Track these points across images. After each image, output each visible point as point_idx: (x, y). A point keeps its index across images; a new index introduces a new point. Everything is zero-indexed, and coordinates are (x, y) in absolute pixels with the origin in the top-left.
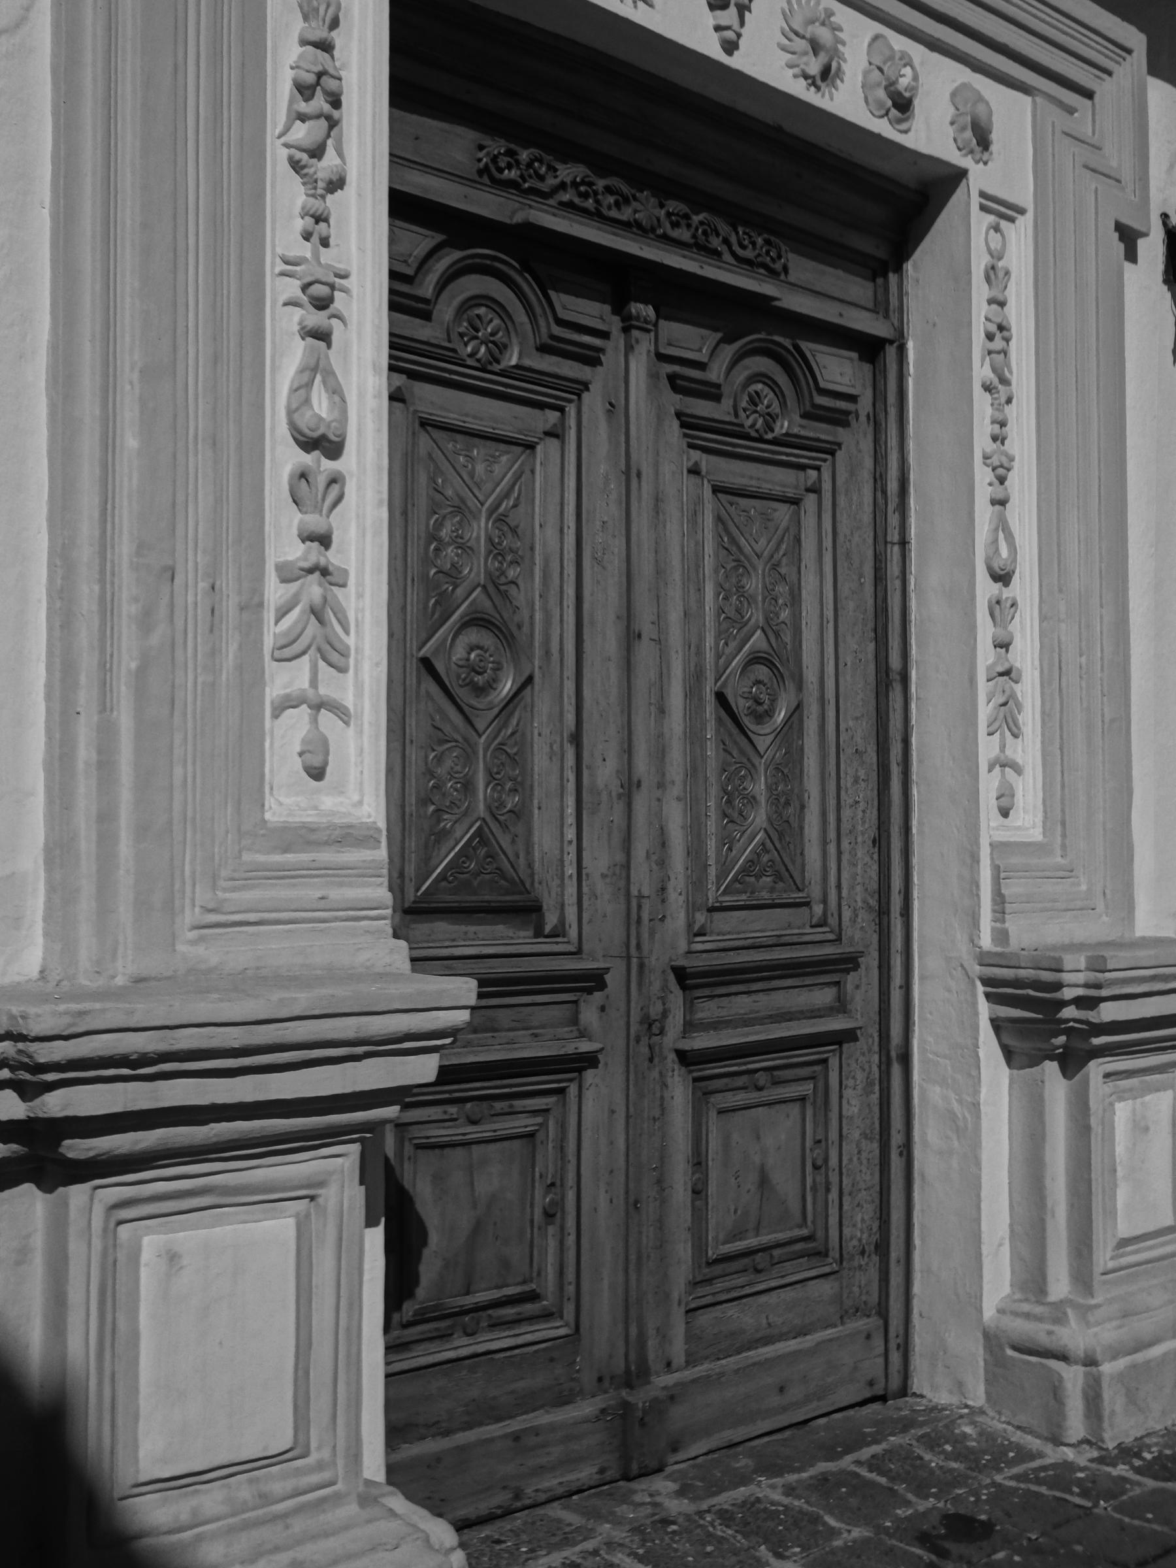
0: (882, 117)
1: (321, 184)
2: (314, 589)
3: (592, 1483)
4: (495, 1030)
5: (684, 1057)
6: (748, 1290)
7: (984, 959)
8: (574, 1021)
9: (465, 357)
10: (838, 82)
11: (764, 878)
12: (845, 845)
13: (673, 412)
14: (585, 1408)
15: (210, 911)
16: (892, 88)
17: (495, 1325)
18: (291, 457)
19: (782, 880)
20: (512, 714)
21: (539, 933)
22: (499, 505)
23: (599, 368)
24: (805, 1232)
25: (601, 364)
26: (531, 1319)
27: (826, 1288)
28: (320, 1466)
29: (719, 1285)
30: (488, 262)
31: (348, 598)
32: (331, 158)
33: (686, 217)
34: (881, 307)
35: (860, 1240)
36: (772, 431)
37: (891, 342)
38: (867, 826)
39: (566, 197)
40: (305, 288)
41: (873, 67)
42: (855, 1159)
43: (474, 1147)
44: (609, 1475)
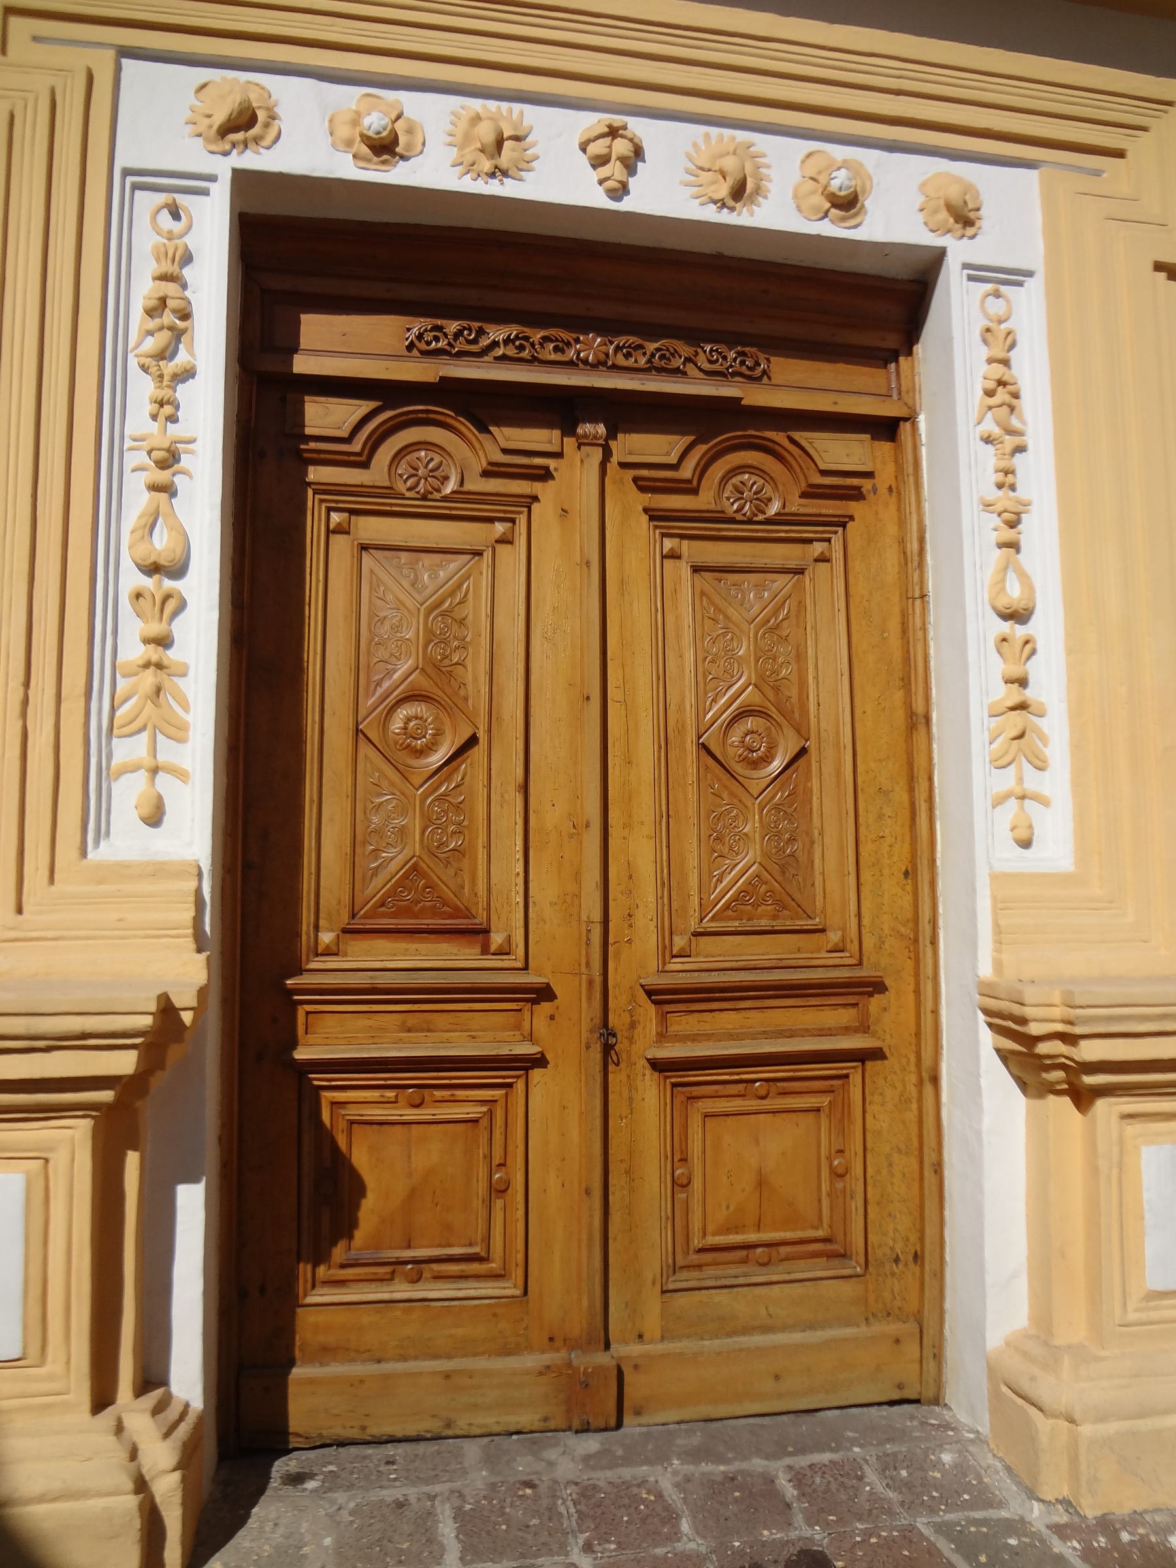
0: (822, 219)
1: (166, 378)
2: (149, 678)
3: (533, 1428)
4: (429, 1030)
5: (659, 1066)
6: (741, 1281)
8: (518, 1027)
9: (404, 491)
10: (760, 199)
11: (763, 907)
12: (866, 876)
13: (640, 508)
14: (531, 1361)
15: (11, 929)
16: (826, 192)
17: (438, 1277)
18: (131, 579)
19: (785, 908)
20: (457, 769)
21: (485, 950)
22: (442, 602)
23: (551, 482)
24: (820, 1233)
25: (552, 478)
26: (477, 1277)
27: (847, 1289)
28: (51, 1378)
29: (710, 1272)
30: (425, 416)
31: (185, 685)
32: (182, 358)
33: (641, 347)
35: (892, 1249)
36: (763, 513)
37: (906, 419)
38: (895, 859)
39: (500, 352)
40: (149, 453)
41: (806, 179)
42: (884, 1172)
43: (414, 1126)
44: (552, 1424)
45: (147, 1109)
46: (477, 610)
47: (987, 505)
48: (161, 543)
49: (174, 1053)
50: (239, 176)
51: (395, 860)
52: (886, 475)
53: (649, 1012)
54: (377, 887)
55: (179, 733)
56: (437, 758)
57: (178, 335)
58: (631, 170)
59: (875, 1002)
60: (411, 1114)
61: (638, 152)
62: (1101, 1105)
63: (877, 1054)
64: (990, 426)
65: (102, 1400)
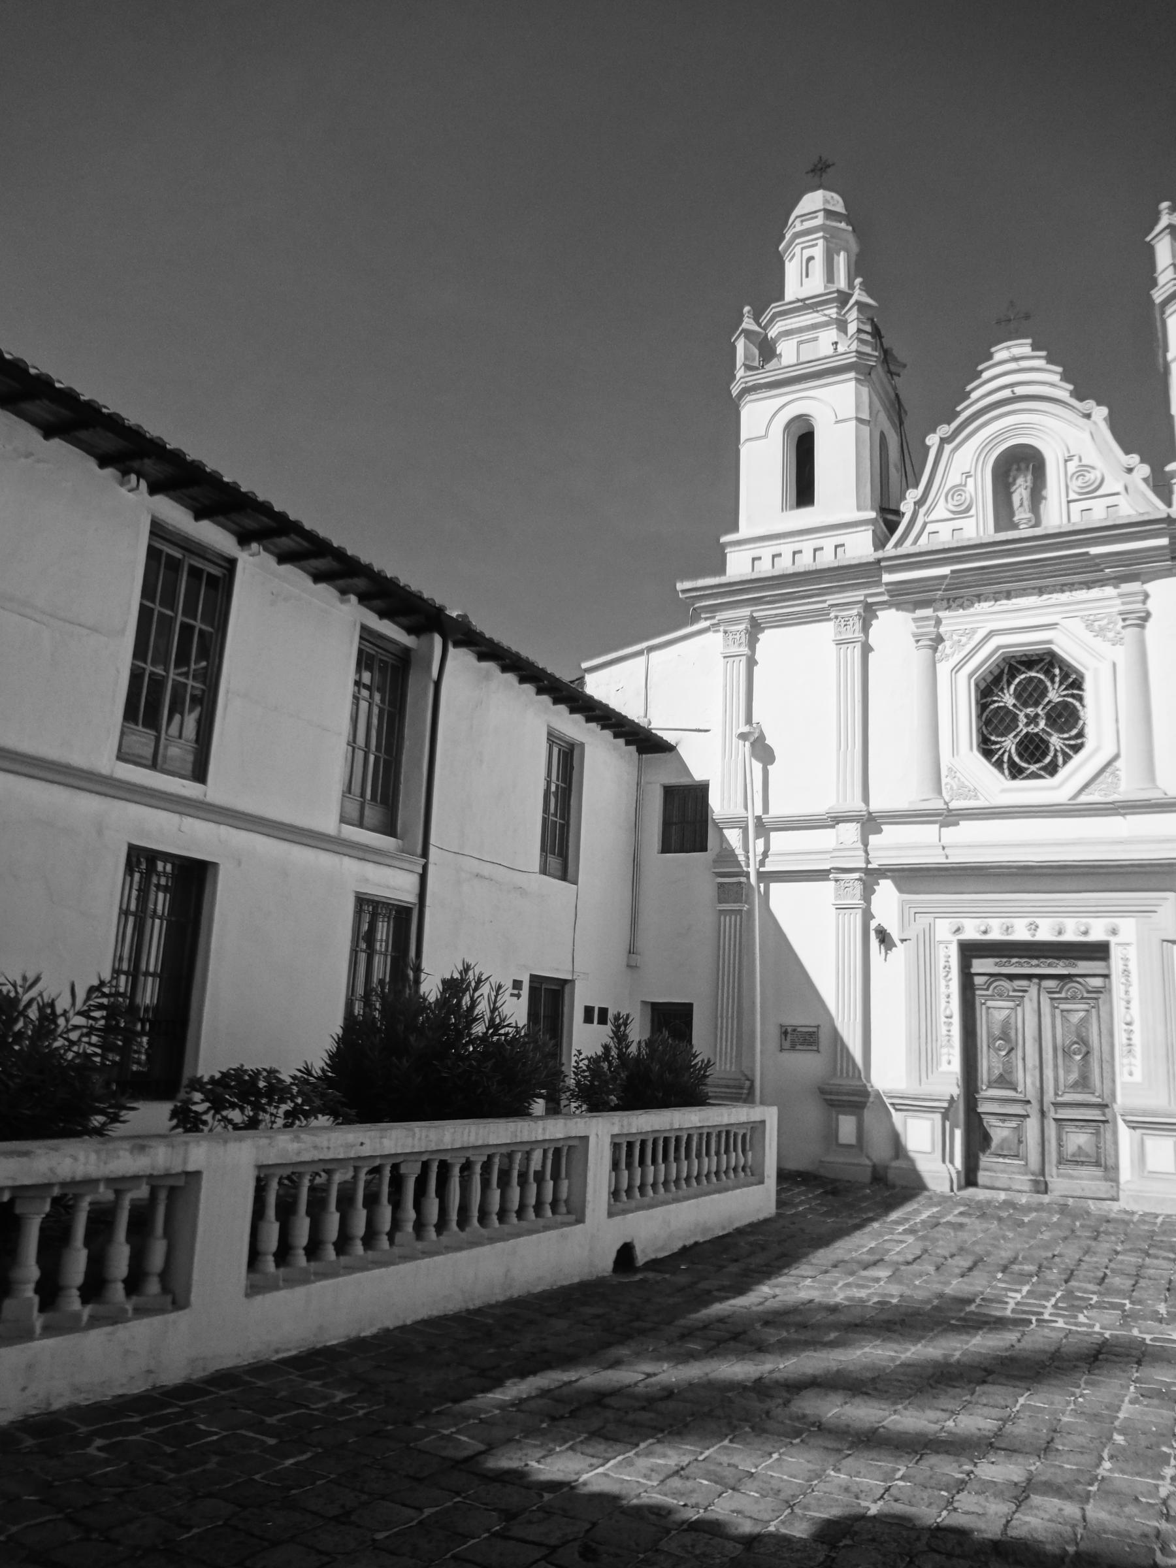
2: (947, 1038)
5: (1055, 1120)
34: (1108, 967)
45: (951, 1115)
46: (1012, 1021)
48: (948, 1013)
49: (954, 1105)
50: (958, 940)
51: (997, 1072)
53: (1052, 1108)
54: (994, 1078)
55: (952, 1047)
56: (1004, 1053)
57: (948, 972)
58: (1035, 930)
59: (1107, 1110)
60: (1000, 1124)
61: (1037, 927)
63: (1106, 1122)
64: (1123, 980)
65: (944, 1161)
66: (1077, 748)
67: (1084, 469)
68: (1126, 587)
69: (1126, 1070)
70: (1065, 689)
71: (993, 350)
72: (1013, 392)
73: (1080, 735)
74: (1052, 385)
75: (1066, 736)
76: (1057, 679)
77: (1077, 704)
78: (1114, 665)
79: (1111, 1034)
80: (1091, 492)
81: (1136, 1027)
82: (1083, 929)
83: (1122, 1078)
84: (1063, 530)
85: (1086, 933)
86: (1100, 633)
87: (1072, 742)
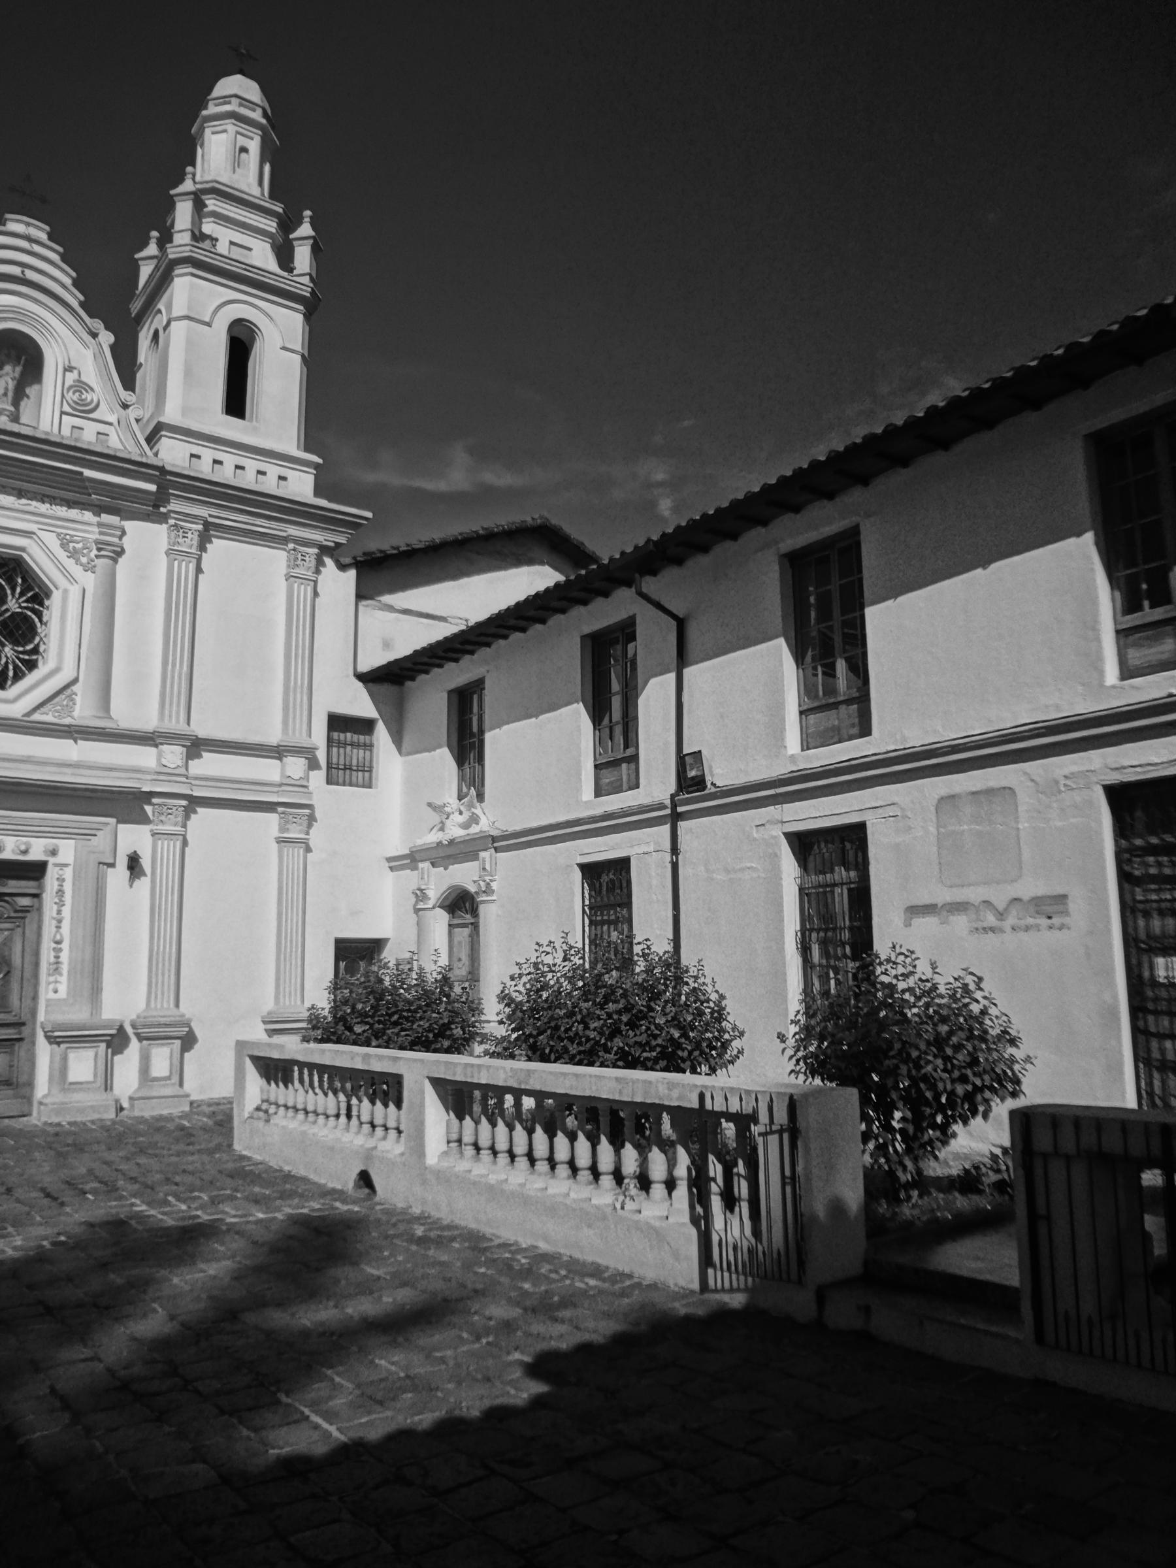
7: (42, 1023)
47: (54, 918)
52: (36, 905)
59: (23, 1028)
62: (62, 1046)
63: (21, 1040)
66: (32, 665)
67: (81, 386)
68: (106, 518)
69: (51, 987)
70: (26, 601)
71: (8, 216)
72: (23, 272)
73: (35, 651)
74: (64, 286)
75: (21, 649)
76: (18, 590)
77: (36, 620)
78: (84, 590)
79: (37, 954)
80: (85, 410)
81: (65, 946)
82: (23, 848)
83: (45, 994)
84: (53, 439)
85: (25, 852)
86: (74, 555)
87: (26, 657)
